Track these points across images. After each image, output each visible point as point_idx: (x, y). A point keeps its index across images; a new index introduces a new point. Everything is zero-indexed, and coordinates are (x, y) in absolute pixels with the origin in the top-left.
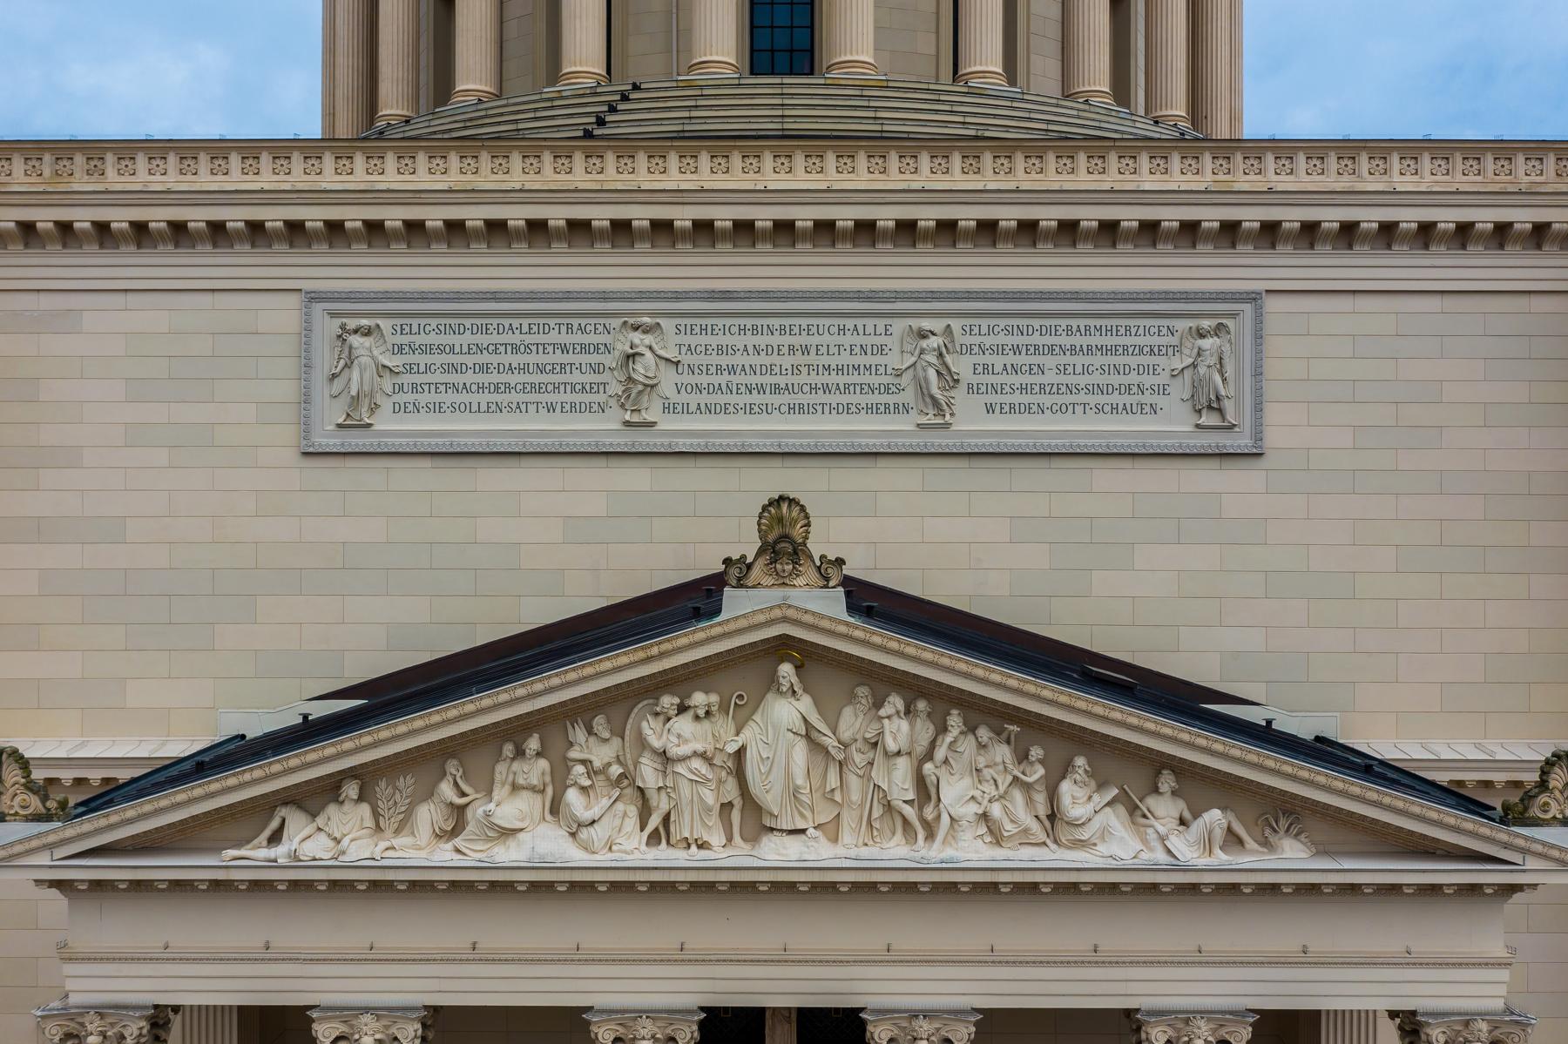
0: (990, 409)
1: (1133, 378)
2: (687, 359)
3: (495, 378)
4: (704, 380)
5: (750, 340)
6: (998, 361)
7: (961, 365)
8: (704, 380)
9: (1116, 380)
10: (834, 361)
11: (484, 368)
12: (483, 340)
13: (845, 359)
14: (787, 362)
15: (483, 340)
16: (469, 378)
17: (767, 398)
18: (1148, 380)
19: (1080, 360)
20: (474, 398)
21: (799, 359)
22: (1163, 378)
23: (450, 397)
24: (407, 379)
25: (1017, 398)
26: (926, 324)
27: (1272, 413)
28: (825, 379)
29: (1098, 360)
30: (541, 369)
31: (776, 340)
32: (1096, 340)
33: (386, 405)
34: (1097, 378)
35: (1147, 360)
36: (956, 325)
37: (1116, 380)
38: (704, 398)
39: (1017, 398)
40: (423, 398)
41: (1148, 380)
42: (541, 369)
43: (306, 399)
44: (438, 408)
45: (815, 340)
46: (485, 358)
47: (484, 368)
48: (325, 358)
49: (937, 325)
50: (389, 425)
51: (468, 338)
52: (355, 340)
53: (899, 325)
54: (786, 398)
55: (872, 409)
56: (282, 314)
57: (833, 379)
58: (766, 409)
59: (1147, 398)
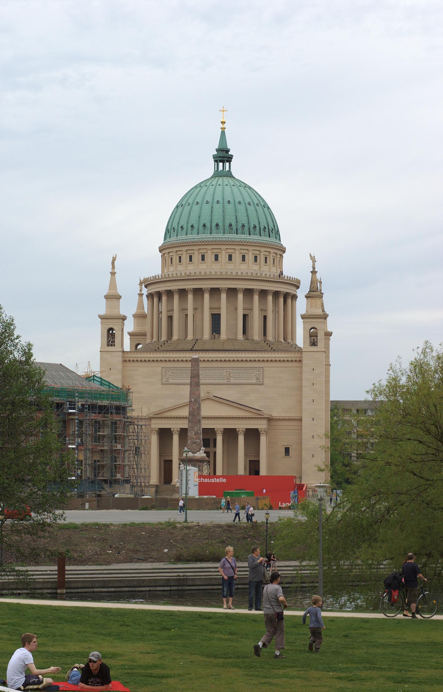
0: (234, 379)
1: (250, 376)
2: (202, 374)
3: (182, 376)
4: (204, 376)
5: (209, 372)
6: (235, 374)
7: (231, 375)
8: (204, 376)
9: (248, 376)
10: (218, 374)
11: (181, 375)
12: (181, 372)
13: (219, 374)
14: (213, 374)
15: (181, 372)
16: (179, 376)
17: (211, 378)
18: (251, 376)
19: (244, 374)
20: (180, 378)
21: (214, 374)
22: (253, 376)
23: (177, 378)
24: (173, 376)
25: (237, 378)
26: (227, 370)
27: (265, 380)
28: (217, 376)
29: (246, 374)
30: (187, 375)
31: (211, 372)
32: (246, 372)
33: (170, 379)
34: (246, 376)
35: (251, 374)
36: (231, 370)
37: (248, 376)
38: (204, 378)
39: (237, 378)
40: (174, 378)
41: (251, 376)
42: (187, 375)
43: (162, 378)
44: (176, 379)
45: (216, 372)
46: (181, 374)
47: (181, 375)
48: (164, 374)
49: (229, 370)
50: (171, 381)
51: (179, 372)
52: (167, 372)
53: (225, 371)
54: (213, 378)
55: (222, 379)
56: (159, 369)
57: (218, 376)
58: (211, 379)
59: (251, 378)
